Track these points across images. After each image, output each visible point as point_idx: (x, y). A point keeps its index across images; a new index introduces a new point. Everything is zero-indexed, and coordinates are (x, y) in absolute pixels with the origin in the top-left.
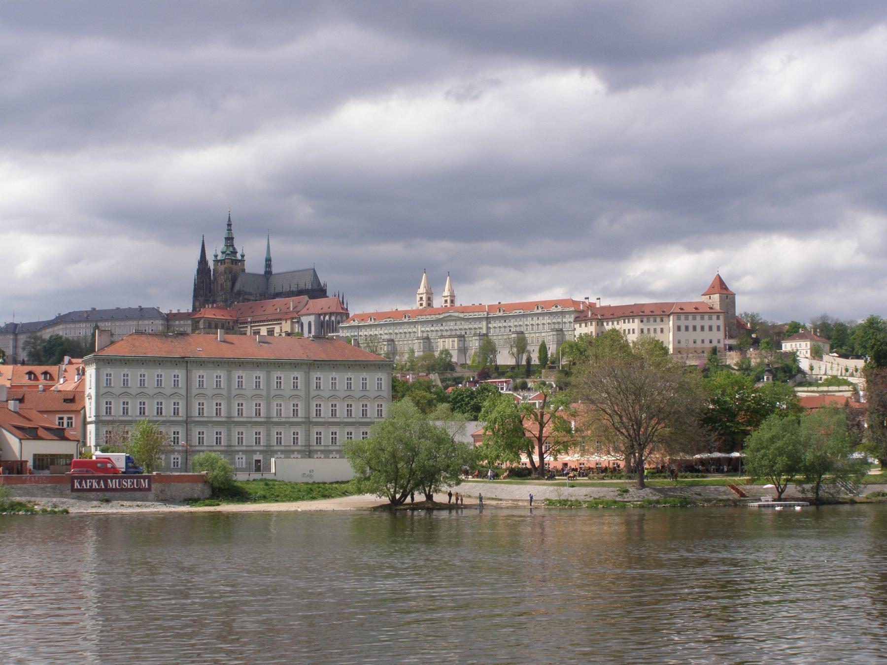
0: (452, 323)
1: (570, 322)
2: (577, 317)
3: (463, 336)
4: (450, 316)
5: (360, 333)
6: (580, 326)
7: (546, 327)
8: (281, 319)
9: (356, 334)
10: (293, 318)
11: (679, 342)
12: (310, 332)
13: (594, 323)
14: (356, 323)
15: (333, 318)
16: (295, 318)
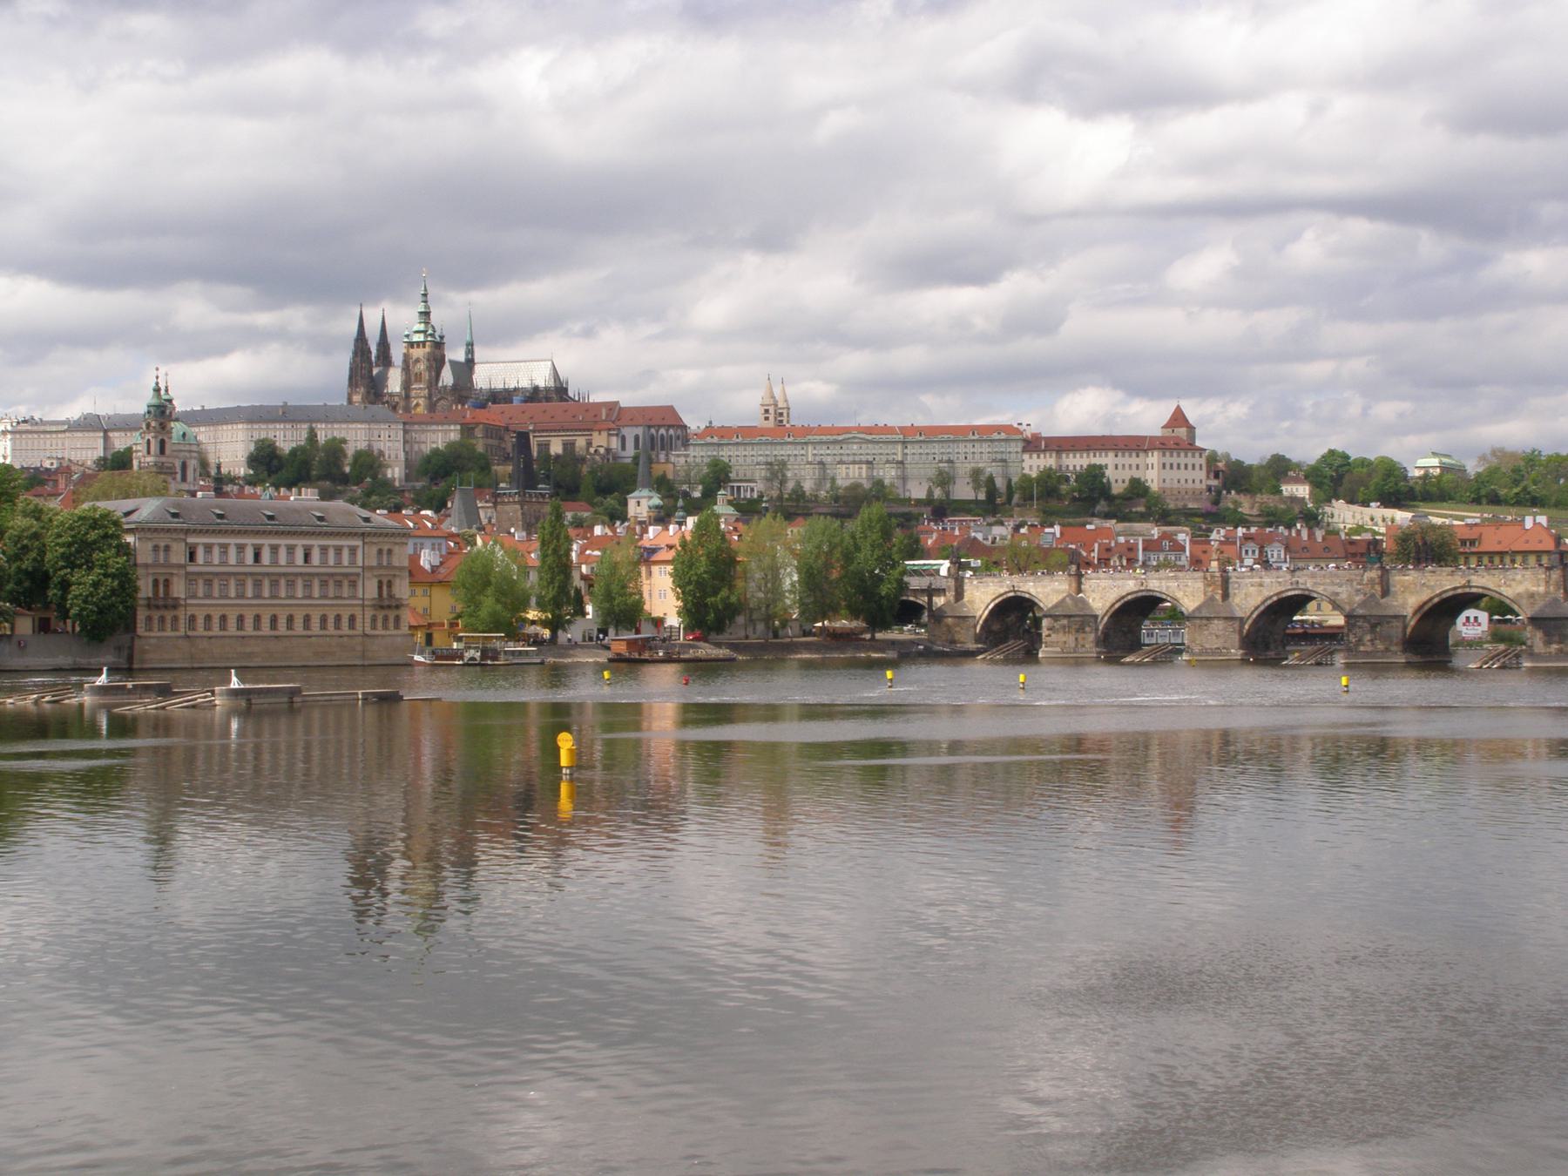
0: (855, 447)
1: (1017, 452)
2: (1024, 447)
3: (868, 462)
4: (854, 438)
5: (721, 453)
6: (1031, 457)
7: (985, 457)
8: (588, 430)
9: (715, 453)
10: (609, 430)
11: (1164, 481)
12: (637, 446)
13: (1054, 455)
14: (716, 440)
15: (671, 432)
16: (614, 430)
